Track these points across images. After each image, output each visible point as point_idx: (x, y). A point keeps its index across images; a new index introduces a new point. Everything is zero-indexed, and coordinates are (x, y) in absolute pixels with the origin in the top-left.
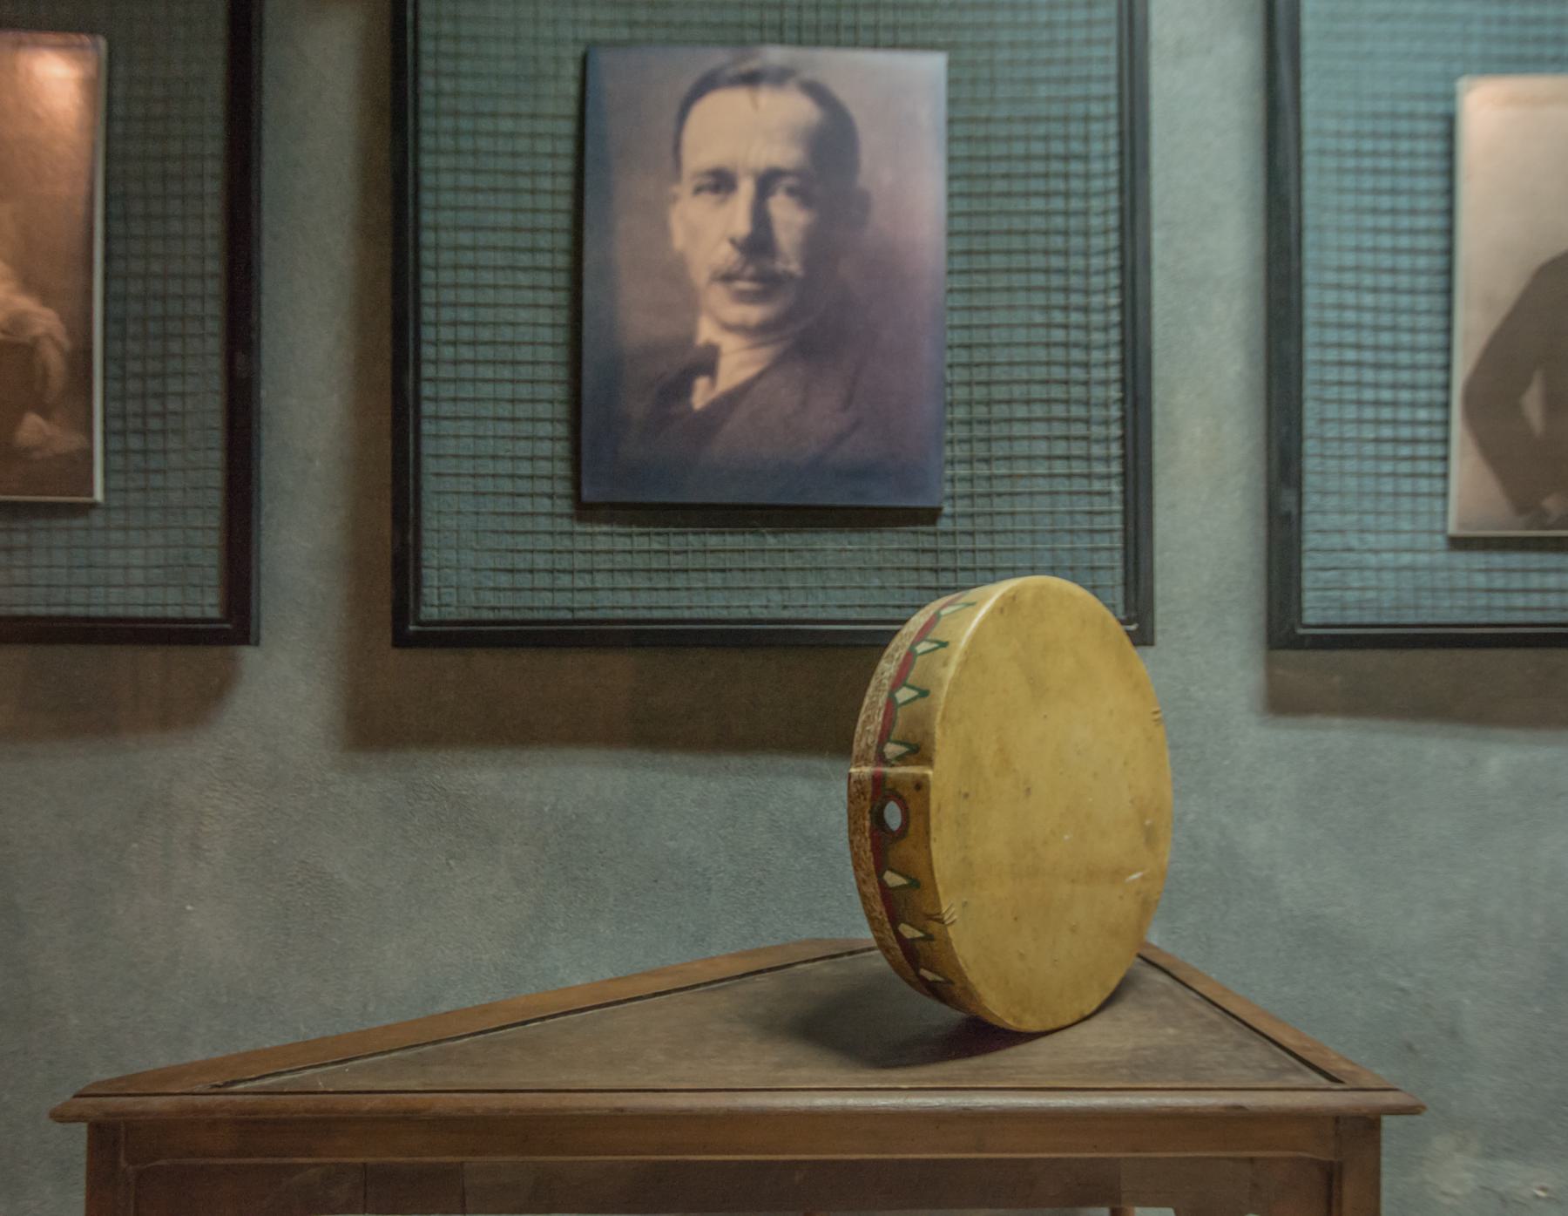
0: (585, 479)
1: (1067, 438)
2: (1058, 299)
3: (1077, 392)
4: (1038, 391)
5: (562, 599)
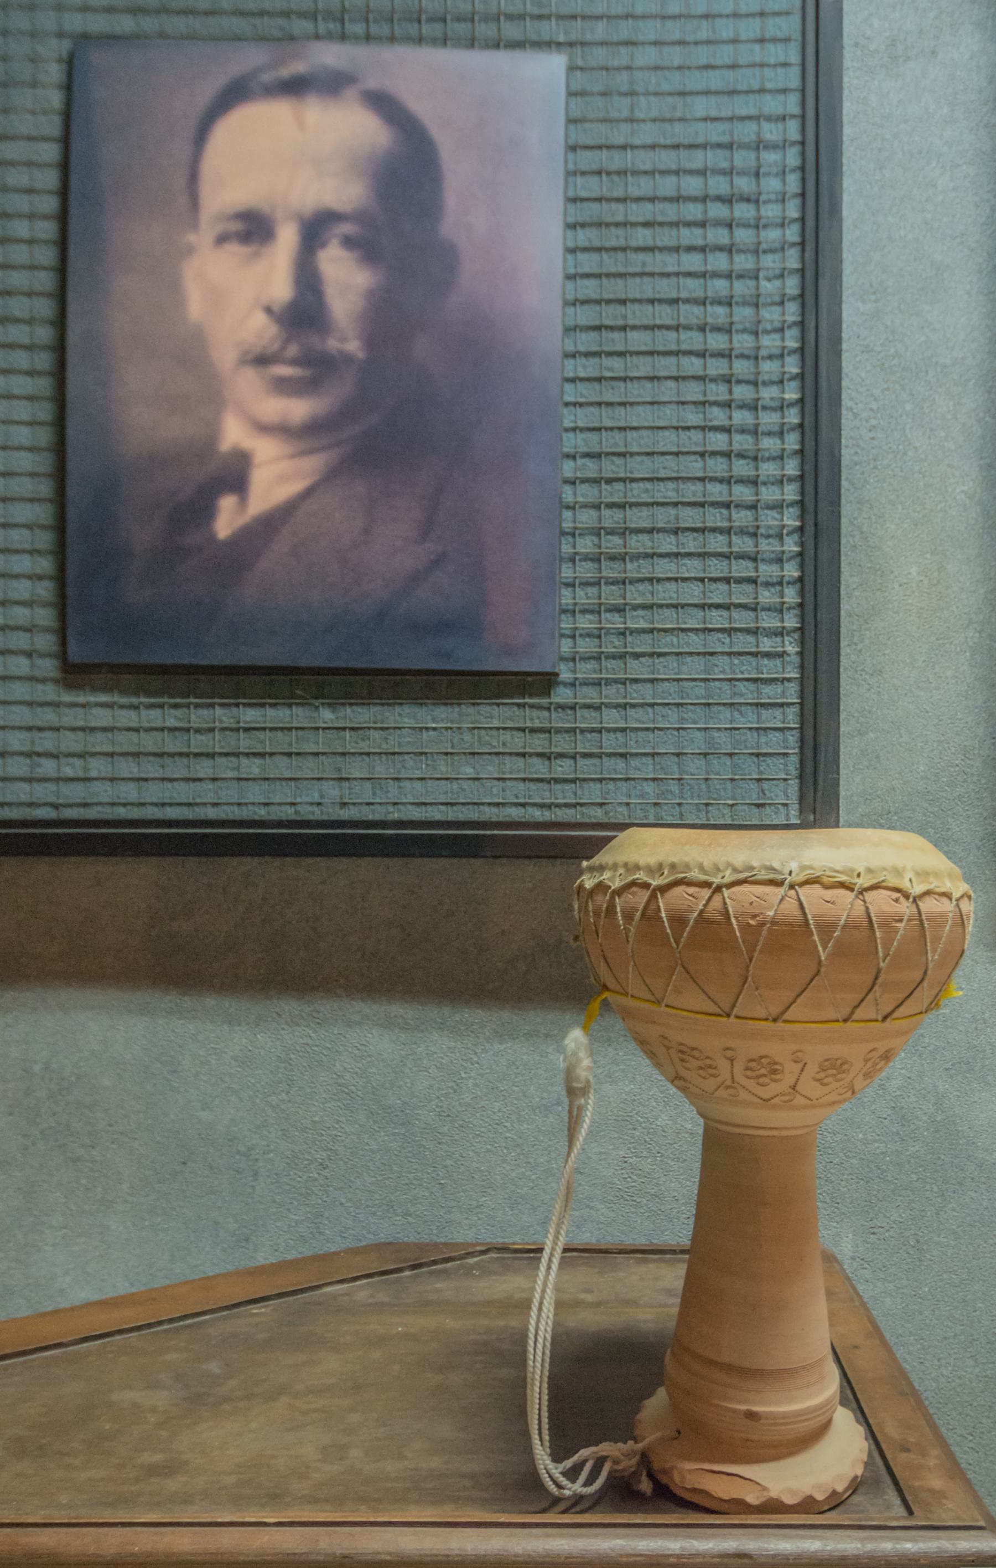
0: (71, 632)
1: (727, 580)
2: (718, 392)
3: (742, 518)
4: (690, 517)
5: (44, 792)
